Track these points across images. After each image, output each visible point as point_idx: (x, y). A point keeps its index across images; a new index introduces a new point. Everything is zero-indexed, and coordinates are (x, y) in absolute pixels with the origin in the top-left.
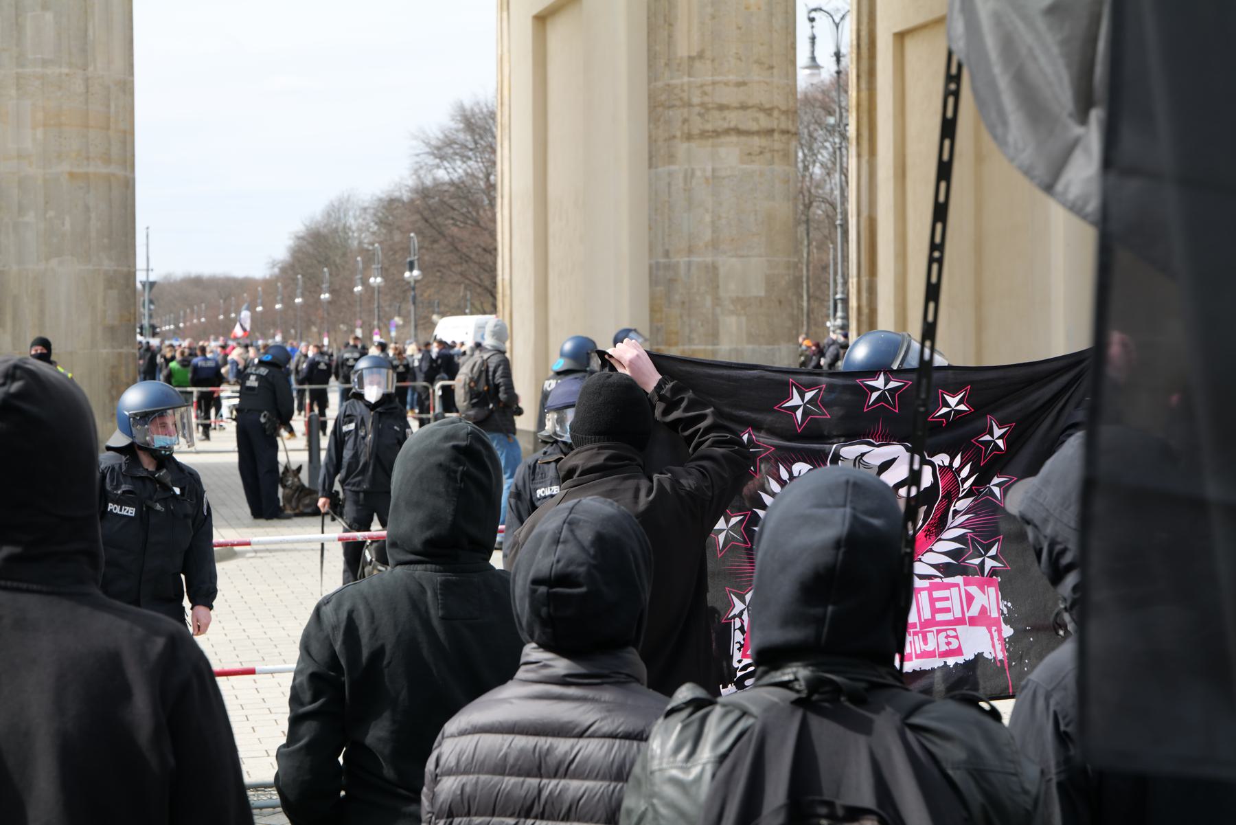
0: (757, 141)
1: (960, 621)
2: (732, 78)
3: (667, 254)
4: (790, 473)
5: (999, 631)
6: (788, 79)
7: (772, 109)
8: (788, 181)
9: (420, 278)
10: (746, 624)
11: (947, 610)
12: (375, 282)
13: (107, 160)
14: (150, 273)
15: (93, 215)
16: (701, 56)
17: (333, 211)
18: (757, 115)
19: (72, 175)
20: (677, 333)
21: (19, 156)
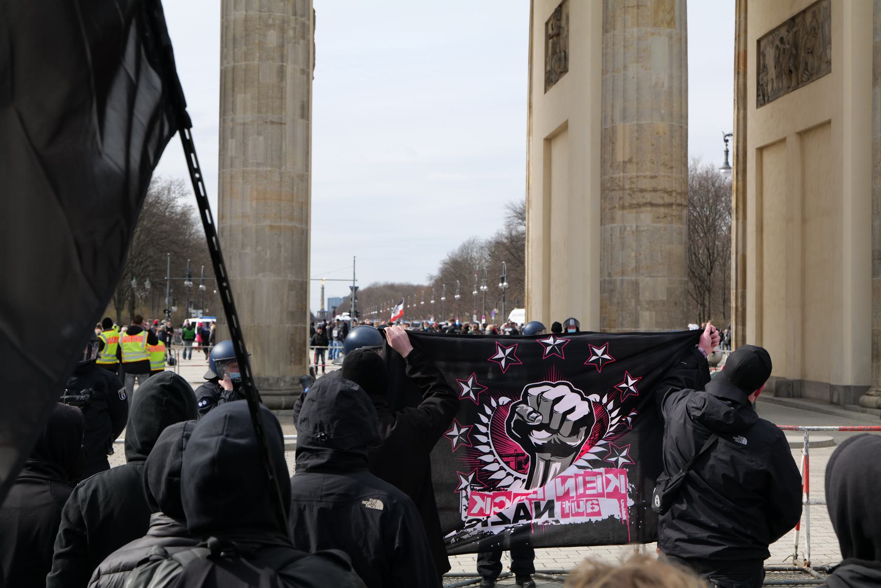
0: (662, 210)
1: (601, 495)
2: (648, 174)
3: (610, 275)
4: (497, 403)
5: (625, 502)
7: (672, 192)
9: (507, 287)
10: (469, 494)
11: (594, 488)
12: (483, 288)
13: (292, 219)
14: (355, 282)
15: (283, 249)
16: (630, 161)
17: (465, 249)
18: (663, 195)
19: (271, 227)
20: (615, 321)
21: (243, 216)
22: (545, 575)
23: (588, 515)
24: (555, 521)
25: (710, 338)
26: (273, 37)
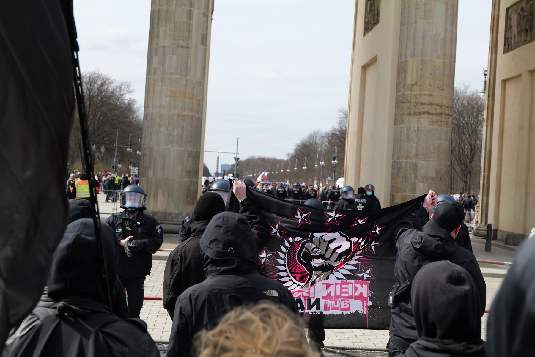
0: (435, 117)
1: (351, 297)
2: (427, 93)
3: (398, 158)
5: (367, 303)
6: (449, 94)
7: (442, 105)
8: (447, 133)
9: (337, 163)
11: (347, 293)
12: (322, 163)
13: (192, 110)
14: (238, 155)
15: (185, 130)
16: (416, 84)
17: (312, 137)
18: (436, 107)
19: (178, 115)
21: (160, 107)
23: (342, 309)
24: (320, 312)
25: (431, 199)
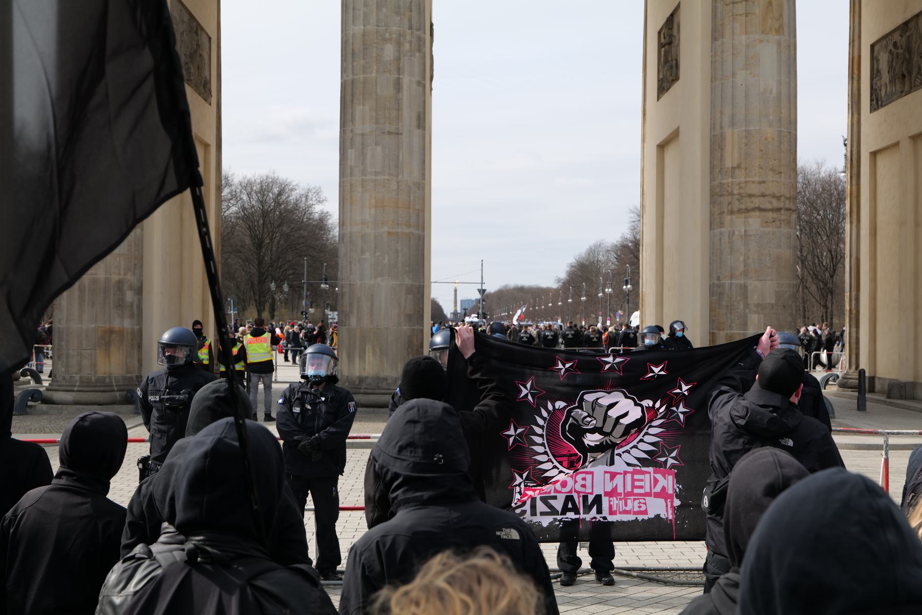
0: (771, 215)
2: (757, 179)
3: (718, 279)
4: (554, 407)
5: (672, 502)
6: (790, 180)
7: (780, 196)
8: (790, 237)
9: (631, 289)
10: (522, 490)
11: (641, 487)
14: (483, 284)
15: (400, 255)
16: (739, 167)
18: (771, 200)
19: (389, 233)
20: (724, 323)
22: (625, 572)
23: (635, 513)
24: (602, 518)
26: (389, 50)
